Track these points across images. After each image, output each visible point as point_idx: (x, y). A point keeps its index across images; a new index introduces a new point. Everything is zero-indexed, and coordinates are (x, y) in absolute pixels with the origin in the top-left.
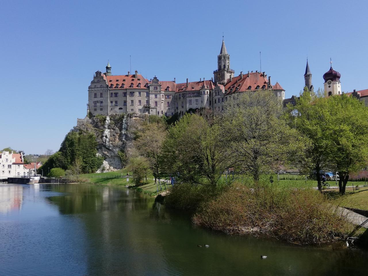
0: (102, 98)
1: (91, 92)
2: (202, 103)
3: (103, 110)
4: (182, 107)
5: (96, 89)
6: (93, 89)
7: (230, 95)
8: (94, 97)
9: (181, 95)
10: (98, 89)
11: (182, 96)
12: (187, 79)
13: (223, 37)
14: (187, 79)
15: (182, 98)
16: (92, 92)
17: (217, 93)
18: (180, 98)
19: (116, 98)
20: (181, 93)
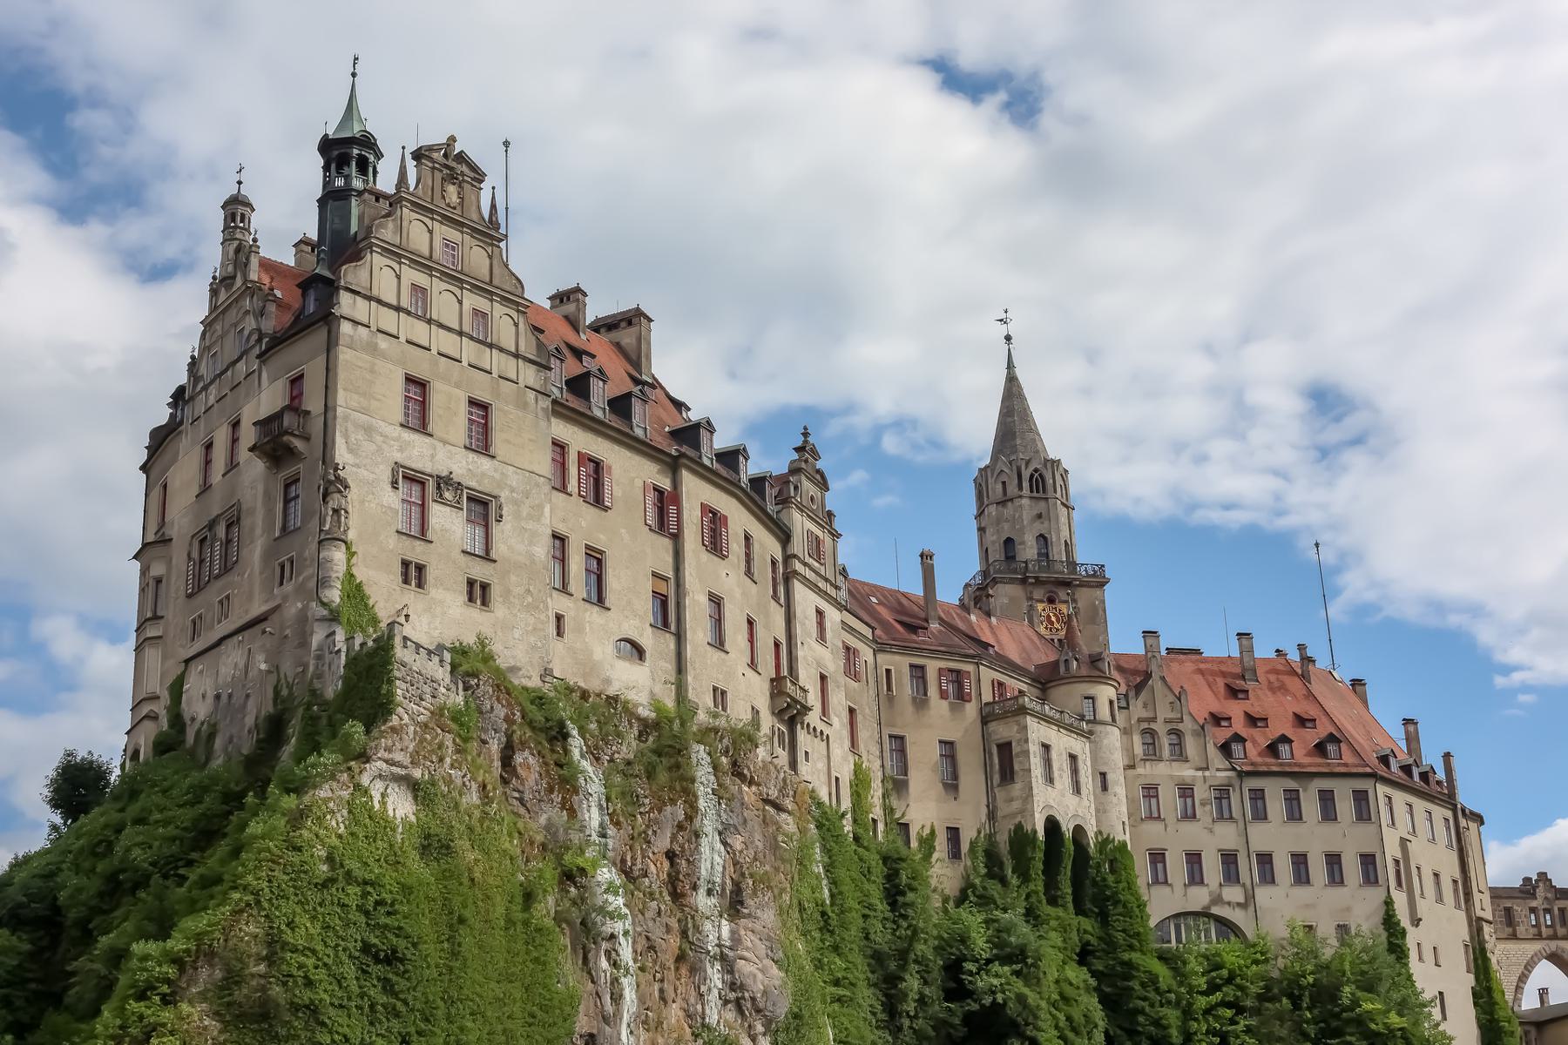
0: (485, 463)
1: (373, 349)
2: (1105, 788)
3: (499, 609)
4: (946, 786)
5: (420, 331)
6: (388, 319)
7: (1291, 784)
8: (399, 417)
9: (931, 675)
10: (448, 343)
11: (943, 695)
12: (926, 557)
13: (1008, 338)
14: (926, 557)
15: (939, 706)
16: (383, 343)
17: (1165, 742)
18: (921, 701)
19: (593, 510)
20: (933, 666)
